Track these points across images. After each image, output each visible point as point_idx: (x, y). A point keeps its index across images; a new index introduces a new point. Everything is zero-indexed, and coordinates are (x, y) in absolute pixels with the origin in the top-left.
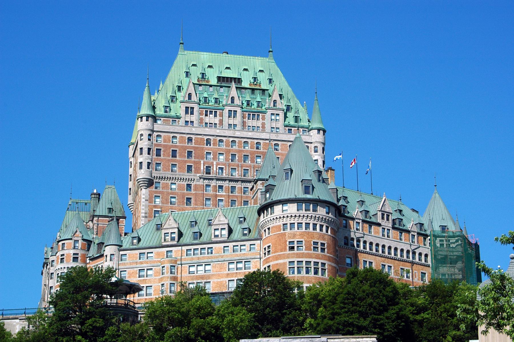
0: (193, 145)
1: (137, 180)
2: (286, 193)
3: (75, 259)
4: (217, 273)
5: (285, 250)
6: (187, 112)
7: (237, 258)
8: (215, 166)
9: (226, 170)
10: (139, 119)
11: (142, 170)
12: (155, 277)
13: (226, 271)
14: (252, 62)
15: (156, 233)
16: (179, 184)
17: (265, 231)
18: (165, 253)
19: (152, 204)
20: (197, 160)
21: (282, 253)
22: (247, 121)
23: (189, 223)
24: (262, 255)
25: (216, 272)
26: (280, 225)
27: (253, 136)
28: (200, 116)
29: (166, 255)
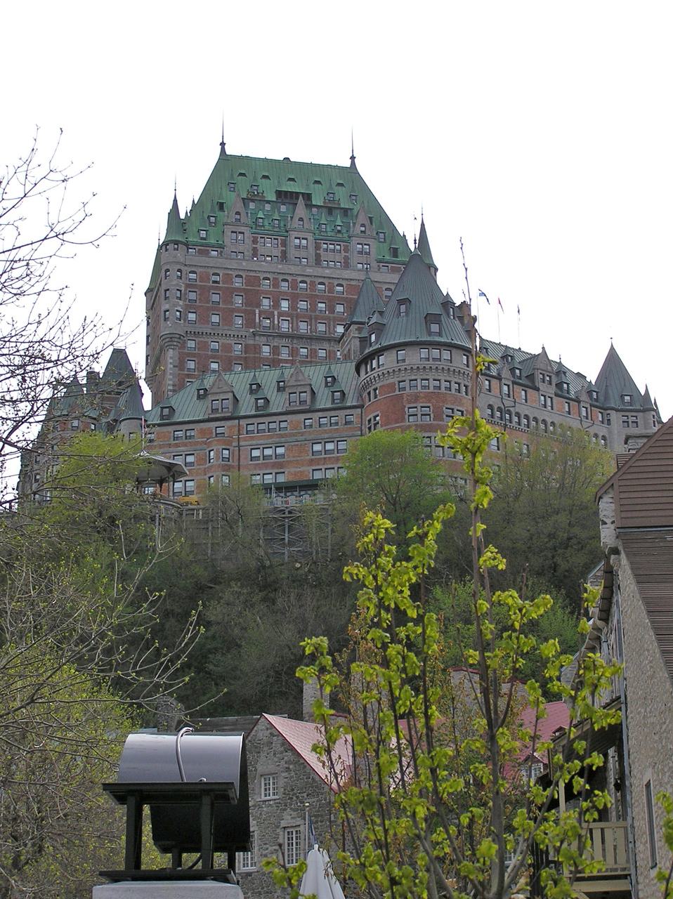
0: (244, 287)
1: (161, 337)
4: (295, 459)
7: (326, 436)
8: (276, 316)
11: (168, 323)
12: (198, 467)
16: (223, 343)
17: (369, 394)
18: (214, 431)
19: (182, 372)
20: (249, 308)
22: (322, 254)
25: (294, 457)
28: (254, 246)
29: (214, 433)
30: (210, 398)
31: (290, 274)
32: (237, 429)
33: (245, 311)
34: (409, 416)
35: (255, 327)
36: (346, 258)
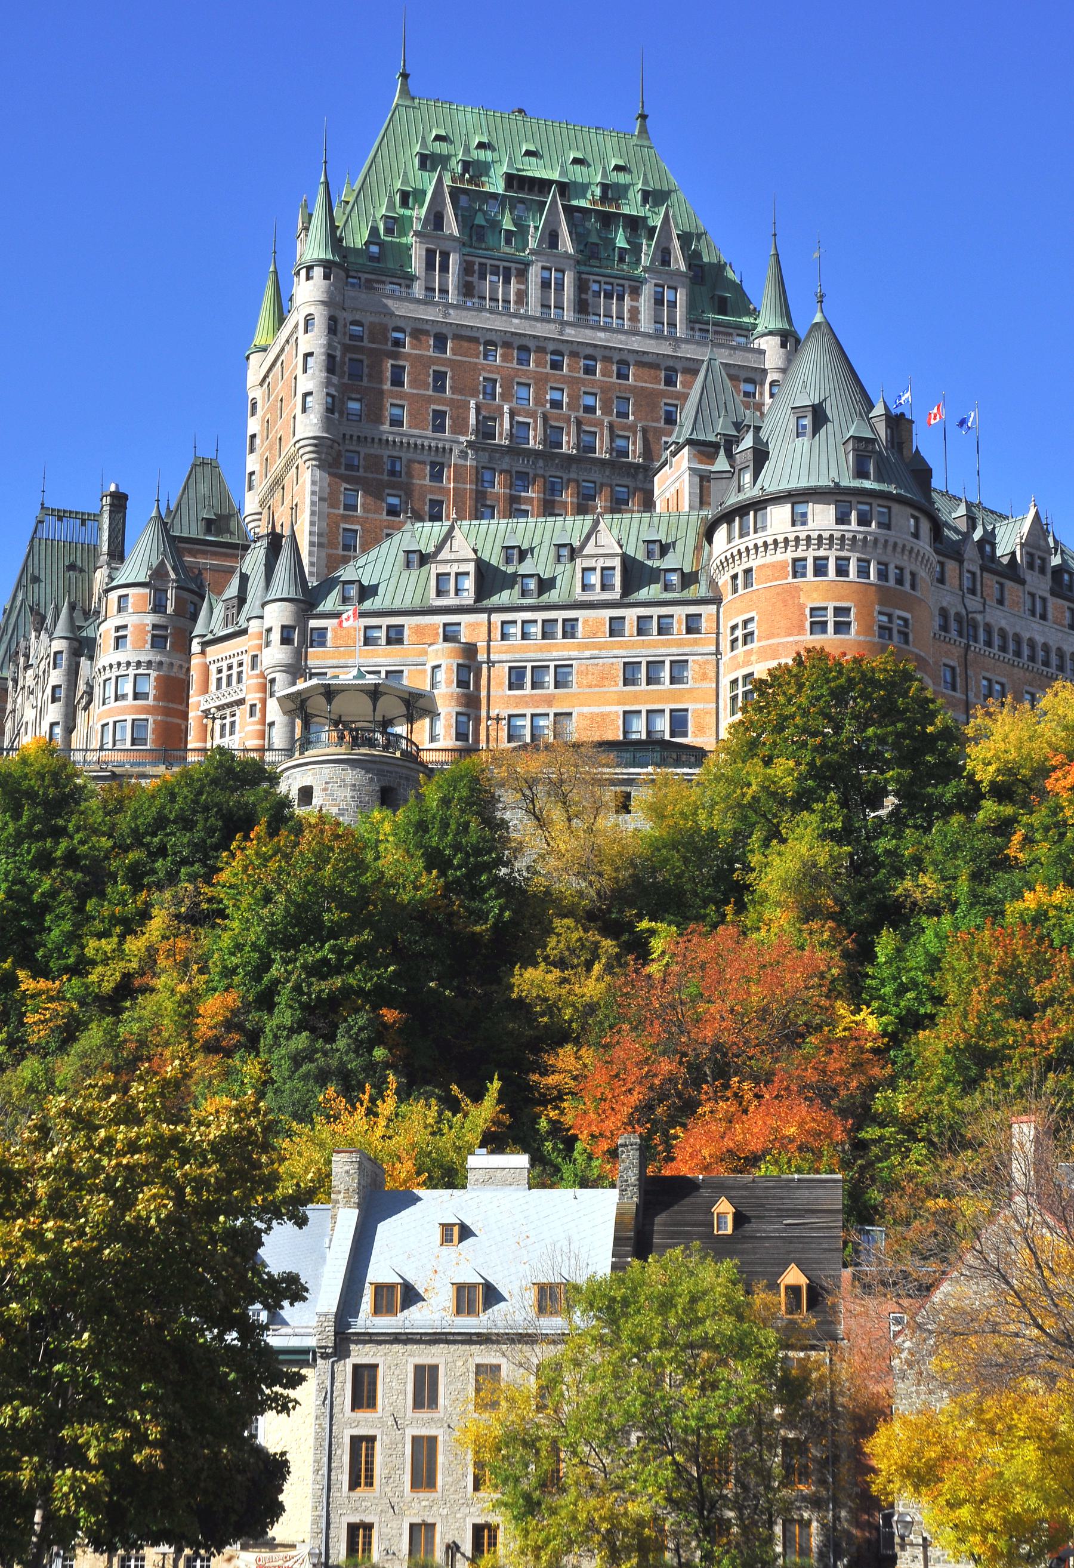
2: (804, 472)
3: (157, 642)
5: (801, 630)
6: (430, 265)
8: (507, 417)
9: (535, 430)
10: (303, 272)
11: (312, 416)
13: (617, 685)
14: (594, 143)
15: (406, 574)
17: (735, 577)
18: (441, 630)
19: (336, 511)
21: (791, 639)
23: (497, 549)
24: (725, 645)
25: (590, 687)
26: (786, 561)
27: (608, 341)
28: (470, 279)
30: (434, 569)
31: (534, 337)
32: (485, 629)
33: (451, 403)
34: (812, 623)
35: (465, 434)
36: (635, 313)
